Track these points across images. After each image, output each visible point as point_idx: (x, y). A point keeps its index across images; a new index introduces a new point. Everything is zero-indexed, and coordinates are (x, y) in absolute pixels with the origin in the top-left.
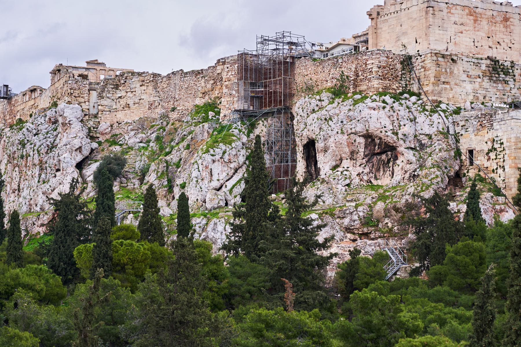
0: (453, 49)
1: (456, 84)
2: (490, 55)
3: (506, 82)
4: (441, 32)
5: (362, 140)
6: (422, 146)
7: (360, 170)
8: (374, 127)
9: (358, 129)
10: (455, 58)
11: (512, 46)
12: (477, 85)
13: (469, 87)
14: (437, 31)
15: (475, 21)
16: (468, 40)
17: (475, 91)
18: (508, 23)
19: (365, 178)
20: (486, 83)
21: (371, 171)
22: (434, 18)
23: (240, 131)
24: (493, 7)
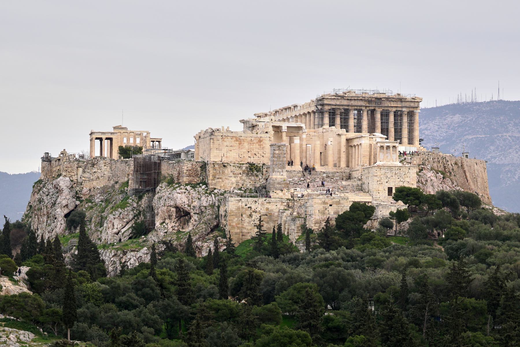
0: (225, 160)
1: (226, 179)
2: (249, 161)
4: (218, 151)
6: (202, 212)
7: (173, 224)
8: (179, 202)
9: (172, 204)
10: (226, 165)
11: (264, 155)
12: (239, 179)
13: (234, 180)
14: (215, 151)
15: (240, 144)
16: (235, 154)
17: (237, 182)
18: (262, 143)
19: (176, 228)
20: (244, 177)
21: (179, 225)
22: (213, 145)
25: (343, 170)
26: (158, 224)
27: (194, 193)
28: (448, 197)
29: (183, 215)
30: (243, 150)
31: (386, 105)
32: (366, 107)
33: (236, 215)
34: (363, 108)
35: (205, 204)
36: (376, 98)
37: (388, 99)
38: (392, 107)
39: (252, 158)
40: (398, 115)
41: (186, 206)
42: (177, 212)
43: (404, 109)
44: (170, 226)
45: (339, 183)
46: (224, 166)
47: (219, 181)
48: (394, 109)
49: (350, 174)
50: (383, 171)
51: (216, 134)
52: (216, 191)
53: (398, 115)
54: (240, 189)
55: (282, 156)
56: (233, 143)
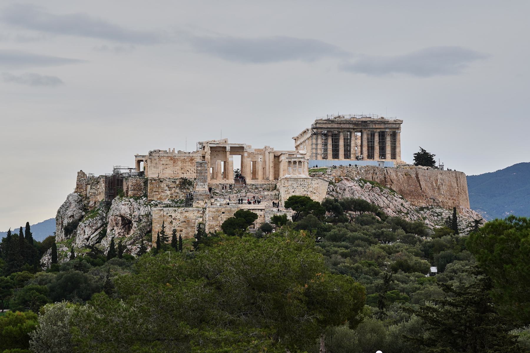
2: (182, 177)
3: (188, 189)
5: (120, 218)
6: (141, 220)
7: (120, 231)
8: (123, 212)
9: (118, 214)
13: (168, 193)
14: (153, 169)
15: (174, 162)
17: (171, 194)
19: (122, 234)
20: (178, 190)
21: (125, 231)
23: (103, 211)
24: (184, 155)
25: (270, 183)
26: (108, 231)
27: (135, 205)
28: (331, 204)
29: (126, 223)
30: (177, 168)
31: (371, 127)
32: (354, 129)
33: (158, 223)
34: (352, 130)
35: (142, 214)
36: (362, 122)
37: (373, 122)
38: (377, 128)
39: (185, 174)
40: (382, 135)
41: (128, 215)
42: (122, 220)
43: (387, 130)
44: (117, 232)
45: (262, 193)
46: (161, 181)
47: (156, 195)
48: (378, 130)
49: (276, 186)
50: (290, 183)
51: (153, 155)
52: (152, 202)
53: (382, 135)
54: (173, 201)
55: (204, 172)
56: (168, 162)
